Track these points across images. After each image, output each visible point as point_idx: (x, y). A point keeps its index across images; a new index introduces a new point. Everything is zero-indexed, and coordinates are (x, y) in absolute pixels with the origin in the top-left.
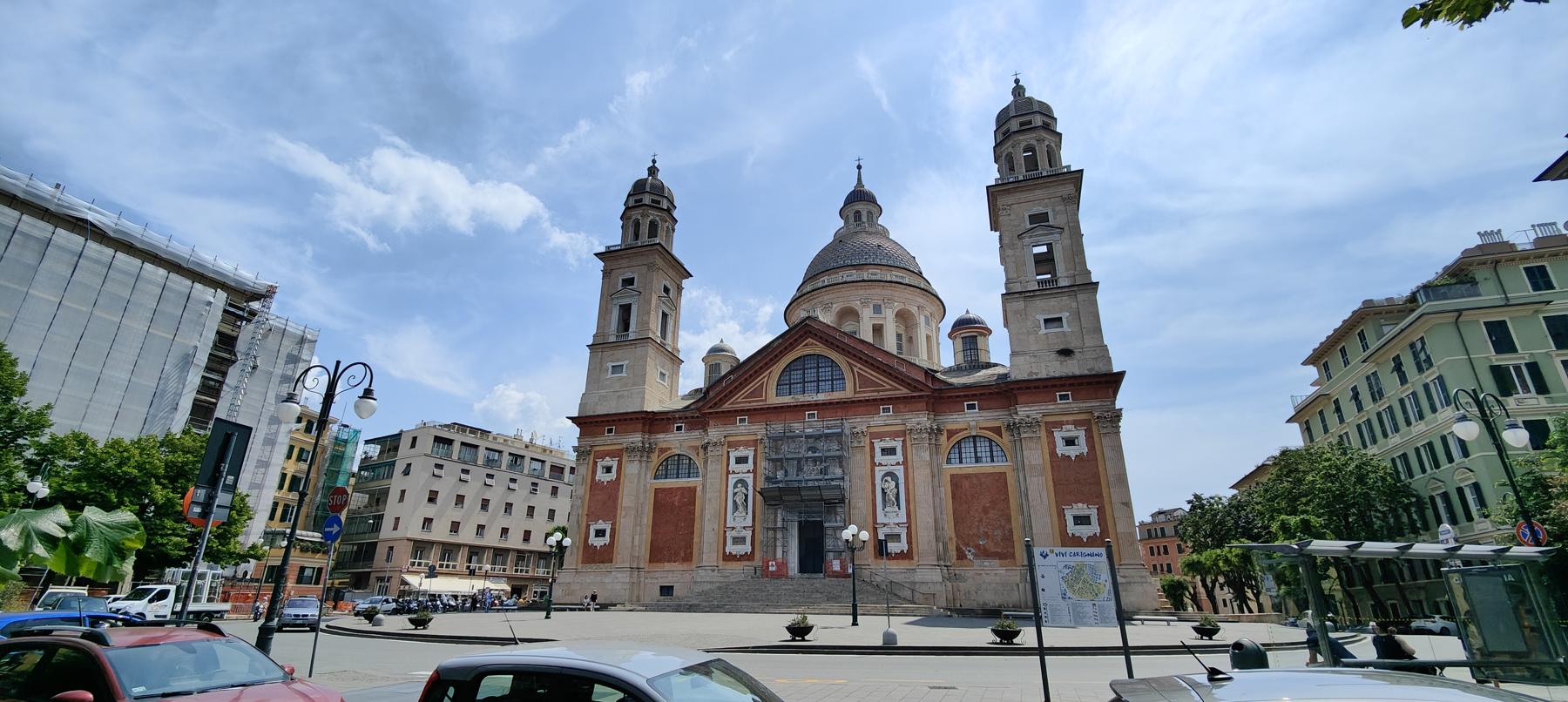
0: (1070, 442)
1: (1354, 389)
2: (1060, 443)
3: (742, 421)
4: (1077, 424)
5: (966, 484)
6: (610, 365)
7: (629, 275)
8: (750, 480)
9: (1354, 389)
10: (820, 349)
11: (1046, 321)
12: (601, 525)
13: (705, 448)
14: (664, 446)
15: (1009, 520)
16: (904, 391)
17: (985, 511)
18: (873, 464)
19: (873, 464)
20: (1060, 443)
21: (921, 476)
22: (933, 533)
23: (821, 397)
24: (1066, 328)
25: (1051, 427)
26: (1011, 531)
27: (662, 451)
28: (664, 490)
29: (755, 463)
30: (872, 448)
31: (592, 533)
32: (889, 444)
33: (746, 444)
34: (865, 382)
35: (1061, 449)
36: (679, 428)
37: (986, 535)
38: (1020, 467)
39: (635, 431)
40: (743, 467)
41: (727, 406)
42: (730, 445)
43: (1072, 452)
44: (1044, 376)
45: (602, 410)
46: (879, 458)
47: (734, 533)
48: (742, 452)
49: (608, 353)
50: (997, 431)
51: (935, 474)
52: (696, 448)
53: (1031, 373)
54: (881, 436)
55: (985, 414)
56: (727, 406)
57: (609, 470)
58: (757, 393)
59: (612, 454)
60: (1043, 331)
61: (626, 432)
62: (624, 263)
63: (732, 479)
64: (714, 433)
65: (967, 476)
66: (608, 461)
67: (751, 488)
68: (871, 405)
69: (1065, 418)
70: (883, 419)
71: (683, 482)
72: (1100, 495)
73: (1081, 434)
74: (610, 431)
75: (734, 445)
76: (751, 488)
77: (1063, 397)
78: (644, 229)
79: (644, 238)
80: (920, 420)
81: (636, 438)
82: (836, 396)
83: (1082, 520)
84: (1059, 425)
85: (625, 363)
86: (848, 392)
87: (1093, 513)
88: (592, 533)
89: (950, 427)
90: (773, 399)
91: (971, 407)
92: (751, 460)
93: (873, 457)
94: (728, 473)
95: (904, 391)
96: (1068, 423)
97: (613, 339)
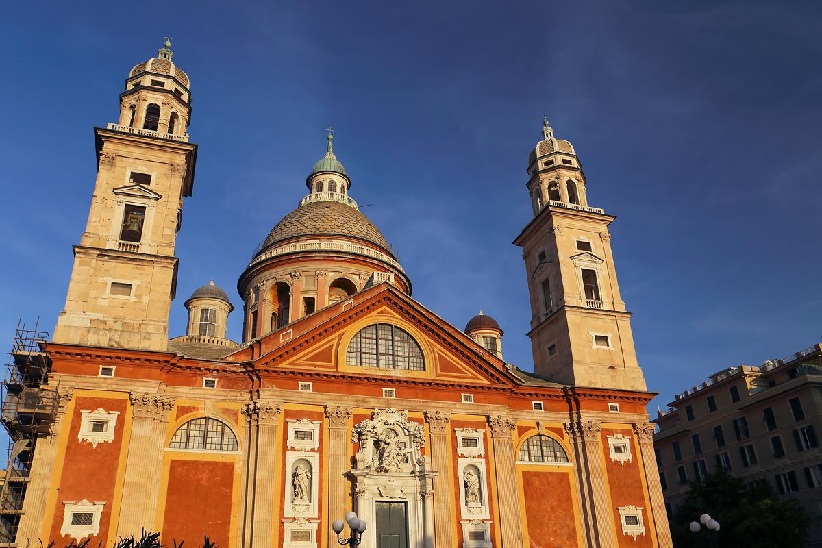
0: (618, 449)
1: (718, 430)
2: (612, 449)
3: (305, 387)
4: (625, 433)
5: (536, 482)
6: (109, 280)
7: (143, 170)
8: (314, 459)
9: (718, 430)
10: (396, 319)
11: (598, 338)
12: (84, 507)
13: (252, 413)
14: (187, 403)
15: (572, 519)
16: (484, 381)
17: (553, 509)
18: (455, 455)
19: (455, 455)
20: (612, 449)
21: (503, 469)
22: (515, 532)
23: (397, 374)
24: (611, 347)
25: (606, 433)
26: (574, 530)
27: (183, 410)
28: (185, 463)
29: (321, 440)
30: (454, 438)
31: (68, 518)
32: (472, 434)
33: (311, 416)
34: (445, 366)
35: (614, 456)
36: (210, 384)
37: (555, 534)
38: (584, 469)
39: (149, 377)
40: (306, 444)
41: (284, 365)
42: (289, 414)
43: (623, 457)
44: (599, 386)
45: (92, 340)
46: (461, 449)
47: (294, 526)
48: (305, 425)
49: (109, 265)
50: (559, 431)
51: (513, 471)
52: (234, 413)
53: (590, 382)
54: (464, 425)
55: (551, 415)
56: (284, 365)
57: (99, 426)
58: (325, 356)
59: (109, 405)
60: (595, 346)
61: (133, 376)
62: (138, 152)
63: (291, 458)
64: (269, 397)
65: (537, 474)
66: (101, 414)
67: (316, 470)
68: (454, 390)
69: (614, 427)
70: (466, 407)
71: (212, 453)
72: (642, 499)
73: (626, 441)
74: (107, 372)
75: (297, 415)
76: (316, 470)
77: (614, 408)
78: (164, 117)
79: (162, 131)
80: (499, 412)
81: (150, 388)
82: (417, 374)
83: (632, 521)
84: (611, 432)
85: (135, 283)
86: (429, 375)
87: (638, 512)
88: (68, 518)
89: (519, 423)
90: (347, 365)
91: (539, 406)
92: (316, 436)
93: (455, 447)
94: (285, 449)
95: (484, 381)
96: (617, 432)
97: (113, 245)
